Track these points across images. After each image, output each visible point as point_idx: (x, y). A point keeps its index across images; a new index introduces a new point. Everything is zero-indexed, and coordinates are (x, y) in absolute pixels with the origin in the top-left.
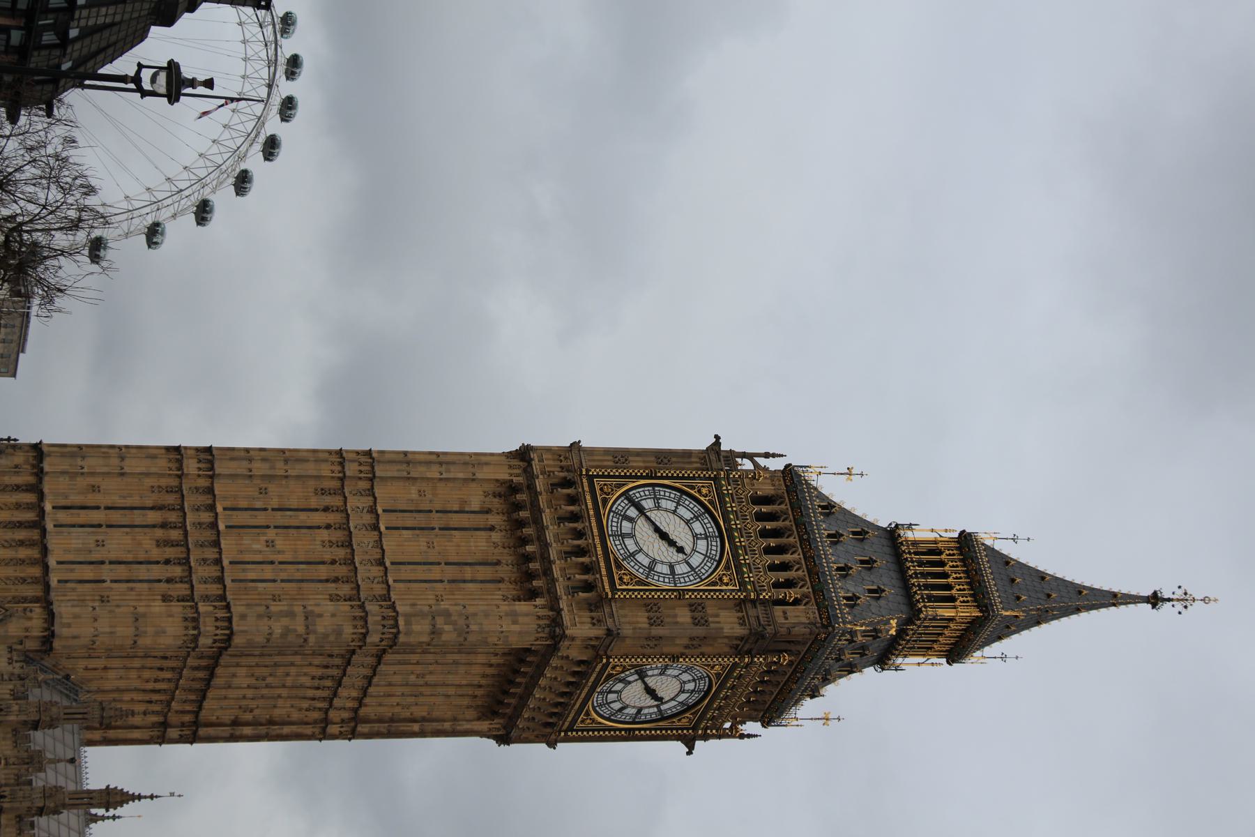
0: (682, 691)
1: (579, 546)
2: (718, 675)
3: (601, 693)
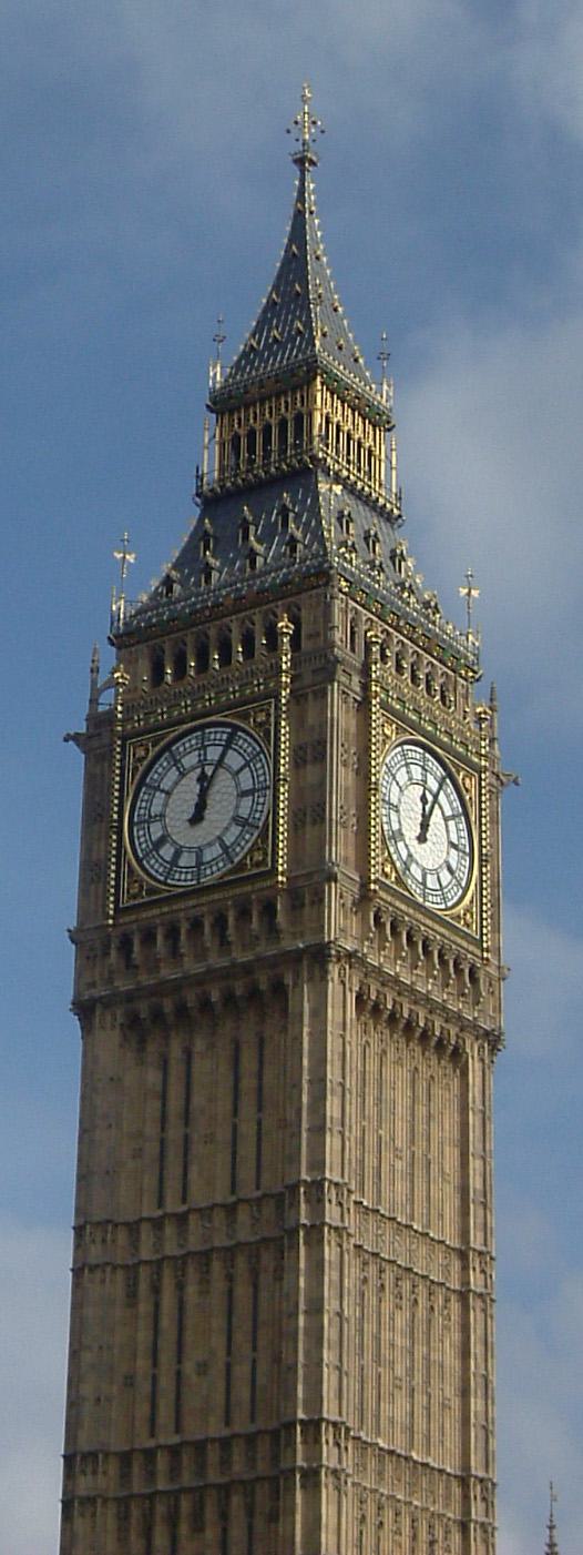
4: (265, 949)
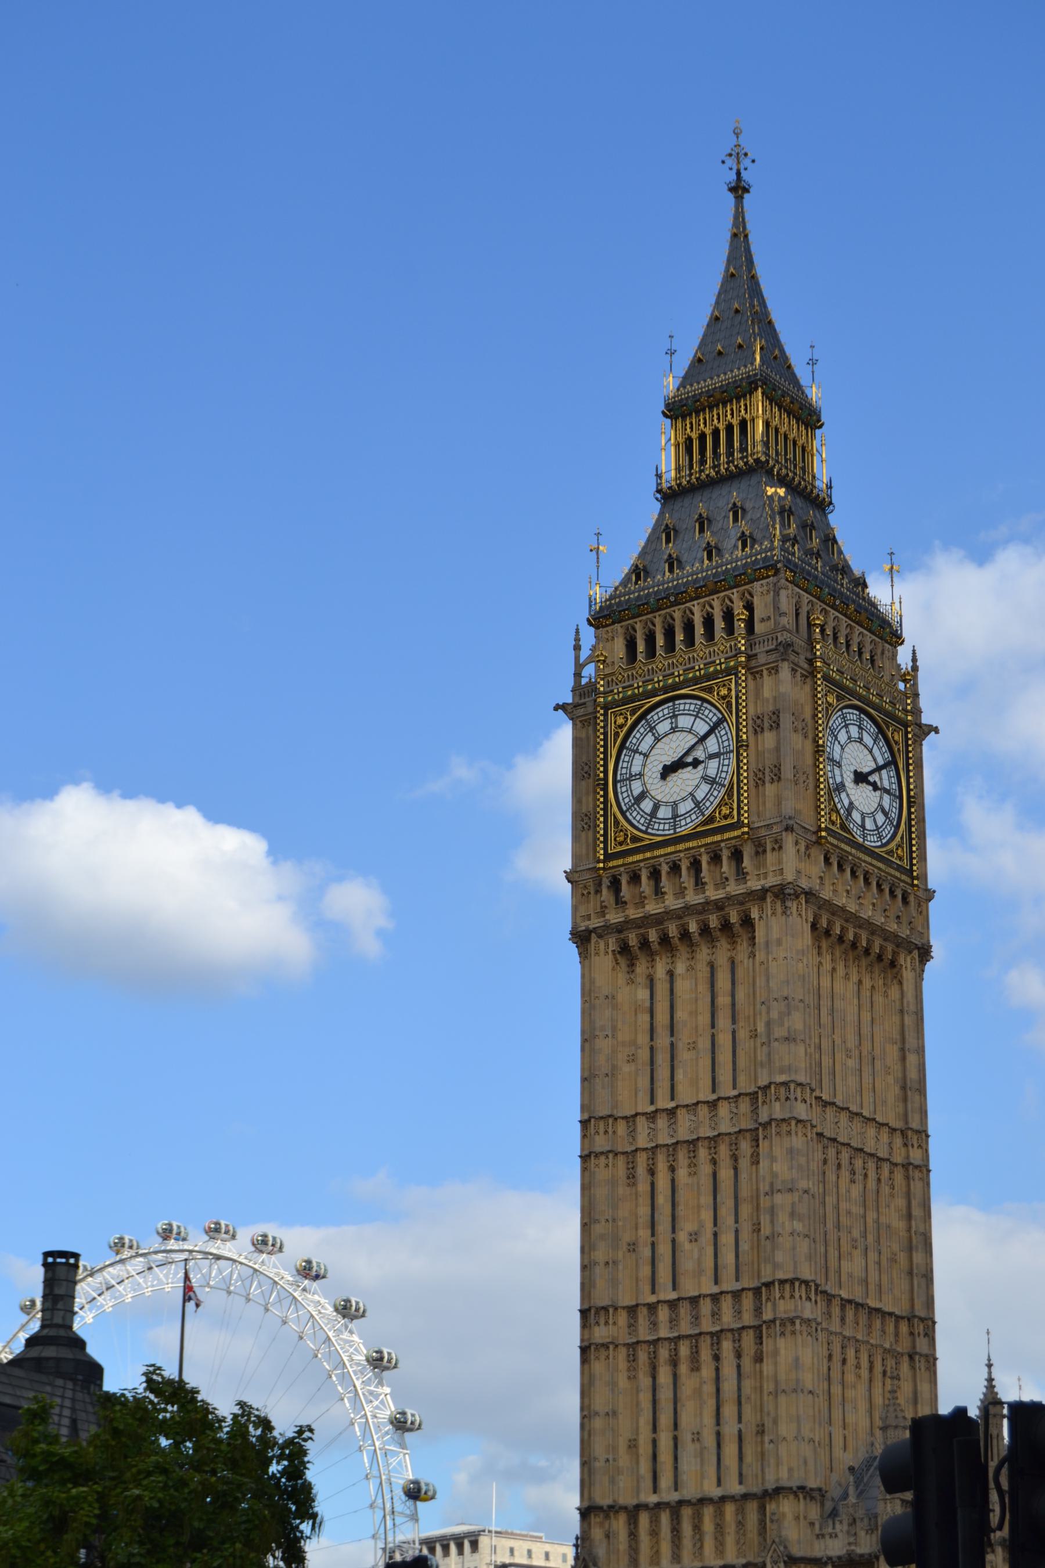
0: (860, 740)
1: (688, 868)
2: (839, 698)
3: (864, 837)
4: (734, 888)
